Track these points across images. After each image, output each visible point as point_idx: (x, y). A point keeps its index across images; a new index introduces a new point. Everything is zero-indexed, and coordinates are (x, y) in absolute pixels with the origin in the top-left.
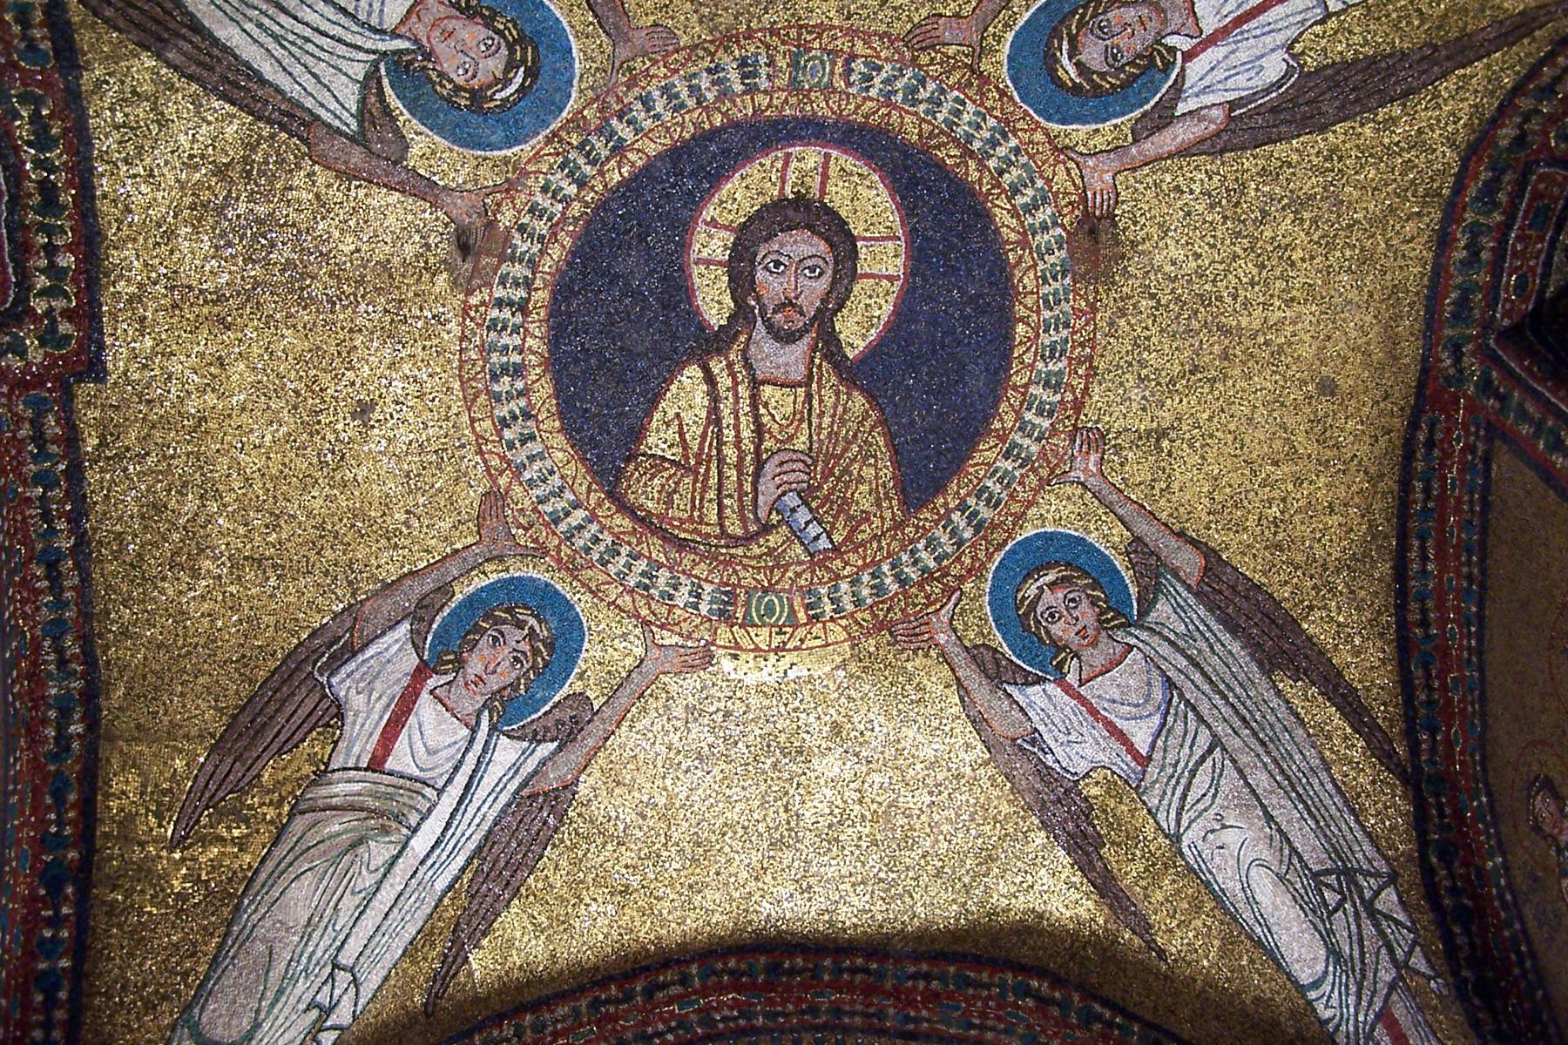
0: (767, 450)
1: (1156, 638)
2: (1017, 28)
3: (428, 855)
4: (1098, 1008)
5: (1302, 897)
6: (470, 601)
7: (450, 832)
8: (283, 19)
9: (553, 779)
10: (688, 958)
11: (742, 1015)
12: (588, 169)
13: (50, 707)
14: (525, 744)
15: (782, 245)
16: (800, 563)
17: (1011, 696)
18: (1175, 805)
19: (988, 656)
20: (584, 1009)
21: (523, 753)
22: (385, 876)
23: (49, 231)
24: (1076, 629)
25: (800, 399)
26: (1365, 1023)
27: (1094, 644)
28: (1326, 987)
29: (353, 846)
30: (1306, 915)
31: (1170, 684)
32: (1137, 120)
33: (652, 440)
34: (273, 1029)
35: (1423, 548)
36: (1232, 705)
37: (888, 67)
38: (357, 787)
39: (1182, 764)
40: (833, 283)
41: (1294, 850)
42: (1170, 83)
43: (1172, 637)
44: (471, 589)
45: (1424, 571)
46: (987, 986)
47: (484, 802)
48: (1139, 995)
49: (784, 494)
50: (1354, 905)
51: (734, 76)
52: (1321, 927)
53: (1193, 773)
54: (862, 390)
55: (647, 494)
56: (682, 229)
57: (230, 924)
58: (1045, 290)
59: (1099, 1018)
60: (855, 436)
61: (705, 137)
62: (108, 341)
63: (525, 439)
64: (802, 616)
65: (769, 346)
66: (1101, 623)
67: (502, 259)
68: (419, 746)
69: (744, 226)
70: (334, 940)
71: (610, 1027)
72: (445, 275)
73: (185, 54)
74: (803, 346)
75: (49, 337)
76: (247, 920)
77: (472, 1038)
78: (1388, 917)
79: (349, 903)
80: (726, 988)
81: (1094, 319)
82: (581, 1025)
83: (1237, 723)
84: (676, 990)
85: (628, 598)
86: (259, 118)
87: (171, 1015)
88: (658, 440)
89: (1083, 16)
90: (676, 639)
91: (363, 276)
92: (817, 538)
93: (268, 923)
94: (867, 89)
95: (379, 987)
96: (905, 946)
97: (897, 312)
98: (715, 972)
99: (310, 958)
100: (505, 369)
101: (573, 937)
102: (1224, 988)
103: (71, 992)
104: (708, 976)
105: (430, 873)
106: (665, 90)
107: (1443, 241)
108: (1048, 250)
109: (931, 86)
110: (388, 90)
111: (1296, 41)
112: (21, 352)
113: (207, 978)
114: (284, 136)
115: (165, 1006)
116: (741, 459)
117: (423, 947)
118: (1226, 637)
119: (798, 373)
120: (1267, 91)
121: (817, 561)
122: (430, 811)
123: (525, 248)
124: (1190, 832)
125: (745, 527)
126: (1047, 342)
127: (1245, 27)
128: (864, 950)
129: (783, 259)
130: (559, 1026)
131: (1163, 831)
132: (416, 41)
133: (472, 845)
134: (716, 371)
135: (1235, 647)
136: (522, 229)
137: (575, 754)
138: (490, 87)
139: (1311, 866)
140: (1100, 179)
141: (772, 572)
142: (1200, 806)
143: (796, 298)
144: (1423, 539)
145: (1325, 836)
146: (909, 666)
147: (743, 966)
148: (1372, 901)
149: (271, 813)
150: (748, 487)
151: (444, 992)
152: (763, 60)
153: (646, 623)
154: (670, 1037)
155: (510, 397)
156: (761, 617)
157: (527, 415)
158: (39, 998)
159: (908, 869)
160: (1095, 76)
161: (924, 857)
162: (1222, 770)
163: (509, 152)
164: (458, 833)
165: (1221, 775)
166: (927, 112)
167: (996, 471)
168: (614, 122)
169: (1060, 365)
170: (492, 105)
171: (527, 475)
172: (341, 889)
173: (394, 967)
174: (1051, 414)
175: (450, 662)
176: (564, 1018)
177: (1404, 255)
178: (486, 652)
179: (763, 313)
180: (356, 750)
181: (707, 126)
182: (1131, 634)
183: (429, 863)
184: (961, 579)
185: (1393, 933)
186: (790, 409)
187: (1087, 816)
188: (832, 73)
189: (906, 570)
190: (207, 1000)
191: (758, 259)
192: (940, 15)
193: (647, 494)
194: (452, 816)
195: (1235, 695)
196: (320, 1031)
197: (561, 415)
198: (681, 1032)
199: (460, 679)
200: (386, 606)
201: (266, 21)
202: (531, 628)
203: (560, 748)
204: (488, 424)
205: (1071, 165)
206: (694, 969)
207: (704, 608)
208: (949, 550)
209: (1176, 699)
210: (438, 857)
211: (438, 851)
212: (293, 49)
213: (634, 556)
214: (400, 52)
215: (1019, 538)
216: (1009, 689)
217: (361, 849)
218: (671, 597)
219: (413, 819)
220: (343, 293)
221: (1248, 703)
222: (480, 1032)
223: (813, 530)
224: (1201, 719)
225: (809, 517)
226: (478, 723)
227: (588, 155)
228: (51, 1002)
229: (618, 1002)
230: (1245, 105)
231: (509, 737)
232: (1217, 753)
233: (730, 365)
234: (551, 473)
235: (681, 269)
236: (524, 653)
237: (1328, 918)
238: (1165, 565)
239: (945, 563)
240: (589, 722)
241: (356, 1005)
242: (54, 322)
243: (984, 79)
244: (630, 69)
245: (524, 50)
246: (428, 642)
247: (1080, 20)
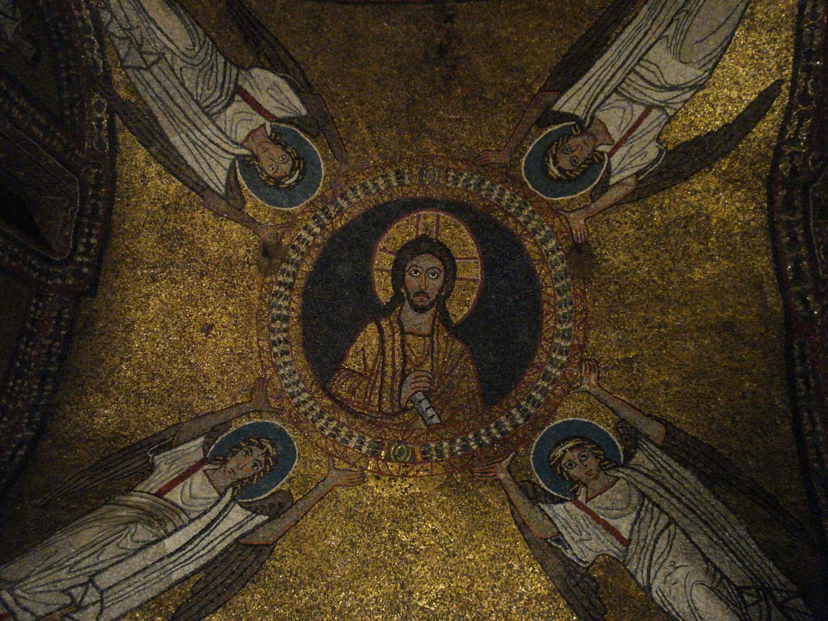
0: (408, 370)
1: (635, 473)
2: (527, 154)
3: (172, 554)
6: (239, 432)
7: (190, 547)
8: (196, 132)
9: (261, 537)
12: (326, 221)
13: (15, 442)
14: (249, 513)
15: (418, 262)
16: (421, 429)
17: (542, 510)
18: (646, 565)
19: (530, 486)
21: (247, 517)
22: (141, 549)
23: (91, 227)
24: (585, 471)
25: (428, 342)
27: (596, 478)
29: (126, 524)
31: (643, 495)
32: (591, 192)
33: (350, 361)
35: (811, 418)
36: (684, 504)
37: (466, 174)
38: (143, 500)
39: (649, 537)
40: (445, 282)
41: (724, 576)
42: (604, 169)
43: (646, 472)
44: (241, 425)
45: (814, 431)
47: (216, 538)
49: (416, 392)
51: (393, 179)
52: (739, 612)
53: (656, 542)
54: (460, 339)
55: (343, 388)
56: (368, 255)
57: (45, 539)
58: (557, 285)
60: (457, 364)
61: (379, 207)
62: (101, 279)
63: (284, 353)
64: (419, 457)
65: (411, 314)
66: (602, 468)
67: (283, 261)
68: (187, 491)
69: (399, 253)
70: (96, 564)
72: (255, 266)
73: (157, 149)
74: (428, 315)
75: (78, 274)
81: (585, 298)
83: (687, 511)
85: (323, 441)
86: (185, 184)
88: (352, 362)
89: (557, 145)
90: (345, 466)
91: (218, 263)
92: (432, 417)
93: (63, 542)
94: (457, 184)
97: (479, 299)
99: (76, 563)
100: (279, 317)
105: (171, 566)
106: (364, 187)
107: (773, 234)
108: (556, 263)
109: (488, 183)
110: (240, 177)
111: (660, 134)
112: (63, 277)
114: (194, 193)
116: (394, 373)
118: (680, 469)
119: (426, 329)
120: (652, 164)
121: (431, 428)
122: (181, 527)
123: (294, 257)
125: (393, 409)
126: (560, 313)
127: (633, 134)
129: (419, 269)
131: (639, 585)
132: (252, 151)
133: (202, 562)
134: (384, 326)
135: (687, 474)
136: (293, 247)
137: (278, 526)
138: (283, 177)
139: (736, 583)
140: (578, 222)
141: (404, 433)
142: (661, 560)
143: (426, 288)
144: (810, 412)
145: (750, 571)
146: (481, 491)
149: (94, 501)
150: (396, 388)
152: (407, 171)
153: (330, 455)
155: (279, 331)
156: (395, 457)
157: (286, 341)
160: (567, 173)
162: (674, 536)
163: (290, 209)
164: (196, 550)
165: (674, 538)
166: (486, 195)
167: (538, 387)
168: (339, 199)
169: (570, 325)
170: (284, 186)
171: (282, 372)
173: (131, 611)
174: (567, 354)
175: (218, 460)
177: (754, 245)
178: (240, 458)
179: (408, 294)
180: (152, 485)
181: (381, 201)
182: (618, 471)
183: (173, 558)
184: (517, 446)
186: (421, 349)
187: (596, 593)
188: (439, 176)
189: (483, 438)
191: (407, 268)
192: (489, 151)
193: (343, 388)
194: (195, 538)
195: (686, 498)
196: (67, 615)
197: (304, 346)
199: (222, 469)
200: (195, 427)
201: (190, 133)
202: (268, 449)
203: (269, 521)
204: (266, 343)
205: (562, 217)
207: (364, 449)
208: (509, 429)
209: (646, 502)
210: (179, 558)
211: (181, 554)
212: (201, 150)
213: (331, 420)
214: (244, 156)
215: (552, 424)
216: (542, 506)
217: (132, 526)
218: (347, 442)
219: (170, 528)
220: (208, 270)
221: (695, 502)
223: (430, 412)
224: (662, 511)
225: (428, 405)
226: (225, 493)
227: (326, 214)
230: (643, 174)
231: (241, 506)
232: (672, 527)
233: (391, 323)
234: (295, 372)
235: (369, 273)
236: (260, 462)
238: (641, 433)
239: (507, 436)
240: (289, 508)
242: (82, 267)
243: (513, 179)
244: (347, 176)
245: (299, 163)
246: (211, 449)
247: (556, 148)
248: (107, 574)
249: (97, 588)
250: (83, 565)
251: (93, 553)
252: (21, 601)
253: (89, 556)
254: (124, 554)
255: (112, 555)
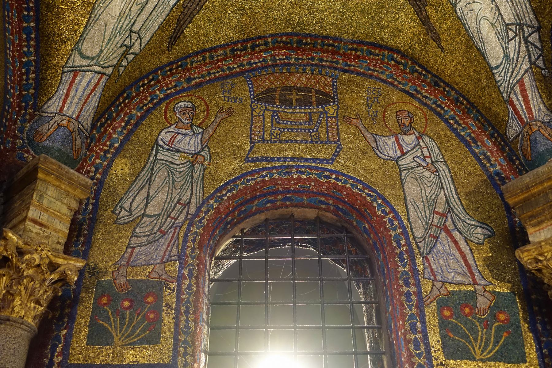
4: (417, 67)
5: (499, 33)
10: (267, 36)
11: (287, 58)
20: (228, 52)
26: (512, 84)
28: (500, 69)
30: (499, 41)
34: (108, 53)
41: (500, 14)
46: (378, 55)
48: (433, 64)
50: (520, 38)
52: (504, 46)
57: (91, 14)
59: (417, 71)
70: (130, 22)
71: (238, 59)
76: (97, 13)
77: (187, 60)
78: (532, 44)
79: (135, 8)
80: (282, 48)
82: (227, 58)
84: (263, 47)
87: (71, 46)
93: (104, 14)
95: (150, 40)
96: (347, 38)
98: (277, 42)
99: (121, 28)
101: (224, 26)
102: (463, 65)
103: (36, 35)
104: (275, 43)
113: (83, 33)
115: (69, 42)
117: (166, 26)
124: (461, 3)
128: (333, 38)
130: (219, 58)
145: (515, 9)
147: (288, 41)
148: (528, 37)
151: (175, 43)
154: (259, 64)
158: (25, 36)
159: (351, 8)
161: (357, 4)
172: (132, 3)
176: (221, 55)
185: (533, 50)
190: (84, 41)
196: (127, 54)
198: (263, 63)
206: (270, 40)
222: (190, 58)
228: (28, 39)
229: (241, 50)
237: (508, 42)
241: (141, 46)
248: (137, 22)
249: (135, 33)
250: (124, 26)
251: (127, 17)
252: (103, 66)
253: (125, 20)
254: (141, 7)
255: (137, 11)
